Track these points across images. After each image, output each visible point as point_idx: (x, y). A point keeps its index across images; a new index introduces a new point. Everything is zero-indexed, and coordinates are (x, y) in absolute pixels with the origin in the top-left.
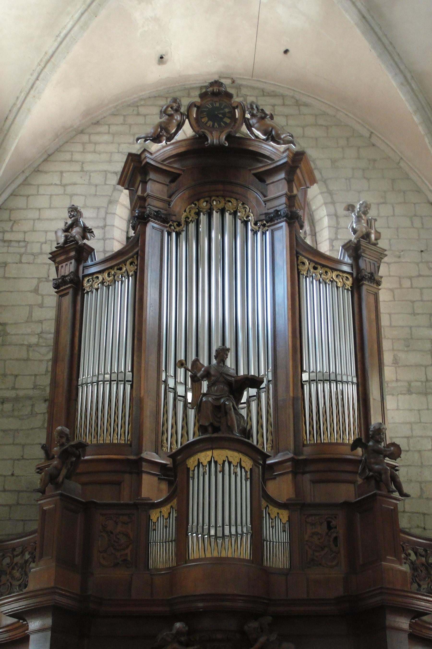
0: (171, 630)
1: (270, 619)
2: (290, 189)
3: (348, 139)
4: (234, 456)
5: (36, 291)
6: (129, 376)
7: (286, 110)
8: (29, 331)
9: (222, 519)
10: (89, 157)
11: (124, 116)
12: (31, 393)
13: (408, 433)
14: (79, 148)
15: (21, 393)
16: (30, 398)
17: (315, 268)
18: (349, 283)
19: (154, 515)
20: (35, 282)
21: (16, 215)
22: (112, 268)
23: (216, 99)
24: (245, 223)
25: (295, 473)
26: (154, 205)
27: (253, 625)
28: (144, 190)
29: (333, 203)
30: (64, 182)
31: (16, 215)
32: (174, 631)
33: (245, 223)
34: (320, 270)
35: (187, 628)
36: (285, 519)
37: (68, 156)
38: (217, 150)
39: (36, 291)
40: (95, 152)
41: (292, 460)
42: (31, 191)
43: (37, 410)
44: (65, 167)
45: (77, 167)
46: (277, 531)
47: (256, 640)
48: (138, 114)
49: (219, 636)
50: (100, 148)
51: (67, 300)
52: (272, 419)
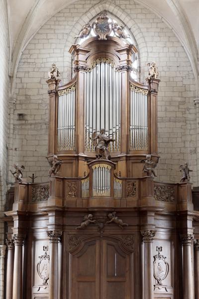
1: (115, 213)
2: (128, 58)
3: (153, 19)
4: (106, 166)
5: (40, 83)
6: (74, 127)
7: (131, 7)
8: (38, 98)
9: (102, 186)
10: (57, 27)
11: (70, 9)
12: (40, 121)
13: (168, 136)
14: (53, 23)
15: (37, 121)
16: (40, 123)
17: (135, 88)
18: (147, 93)
19: (83, 181)
20: (40, 79)
21: (31, 52)
22: (67, 88)
23: (103, 20)
24: (113, 68)
25: (127, 160)
26: (81, 64)
28: (78, 58)
29: (147, 47)
30: (48, 38)
31: (31, 52)
33: (113, 68)
34: (137, 89)
36: (121, 183)
37: (49, 27)
38: (104, 41)
39: (40, 83)
40: (58, 25)
41: (126, 156)
42: (36, 42)
43: (43, 127)
44: (48, 31)
45: (53, 32)
46: (118, 185)
48: (75, 8)
49: (101, 217)
50: (61, 23)
51: (53, 98)
52: (120, 141)
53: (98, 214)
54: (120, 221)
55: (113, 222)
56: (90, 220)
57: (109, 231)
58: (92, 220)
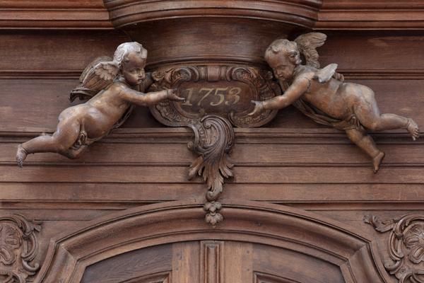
0: (112, 56)
27: (284, 48)
32: (117, 61)
35: (144, 54)
47: (290, 80)
49: (213, 71)
53: (187, 46)
54: (361, 93)
55: (304, 111)
56: (122, 89)
57: (276, 176)
58: (147, 90)
